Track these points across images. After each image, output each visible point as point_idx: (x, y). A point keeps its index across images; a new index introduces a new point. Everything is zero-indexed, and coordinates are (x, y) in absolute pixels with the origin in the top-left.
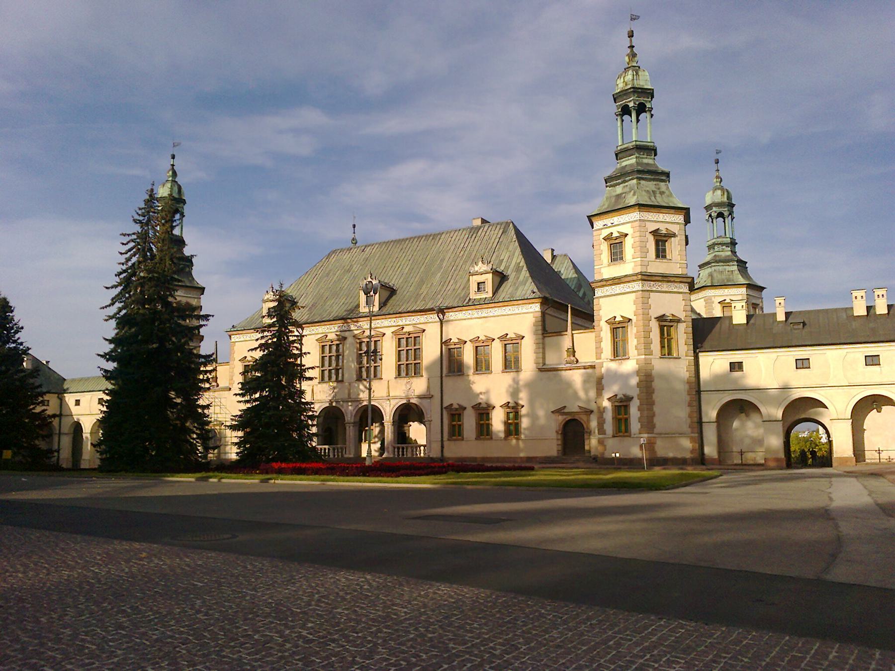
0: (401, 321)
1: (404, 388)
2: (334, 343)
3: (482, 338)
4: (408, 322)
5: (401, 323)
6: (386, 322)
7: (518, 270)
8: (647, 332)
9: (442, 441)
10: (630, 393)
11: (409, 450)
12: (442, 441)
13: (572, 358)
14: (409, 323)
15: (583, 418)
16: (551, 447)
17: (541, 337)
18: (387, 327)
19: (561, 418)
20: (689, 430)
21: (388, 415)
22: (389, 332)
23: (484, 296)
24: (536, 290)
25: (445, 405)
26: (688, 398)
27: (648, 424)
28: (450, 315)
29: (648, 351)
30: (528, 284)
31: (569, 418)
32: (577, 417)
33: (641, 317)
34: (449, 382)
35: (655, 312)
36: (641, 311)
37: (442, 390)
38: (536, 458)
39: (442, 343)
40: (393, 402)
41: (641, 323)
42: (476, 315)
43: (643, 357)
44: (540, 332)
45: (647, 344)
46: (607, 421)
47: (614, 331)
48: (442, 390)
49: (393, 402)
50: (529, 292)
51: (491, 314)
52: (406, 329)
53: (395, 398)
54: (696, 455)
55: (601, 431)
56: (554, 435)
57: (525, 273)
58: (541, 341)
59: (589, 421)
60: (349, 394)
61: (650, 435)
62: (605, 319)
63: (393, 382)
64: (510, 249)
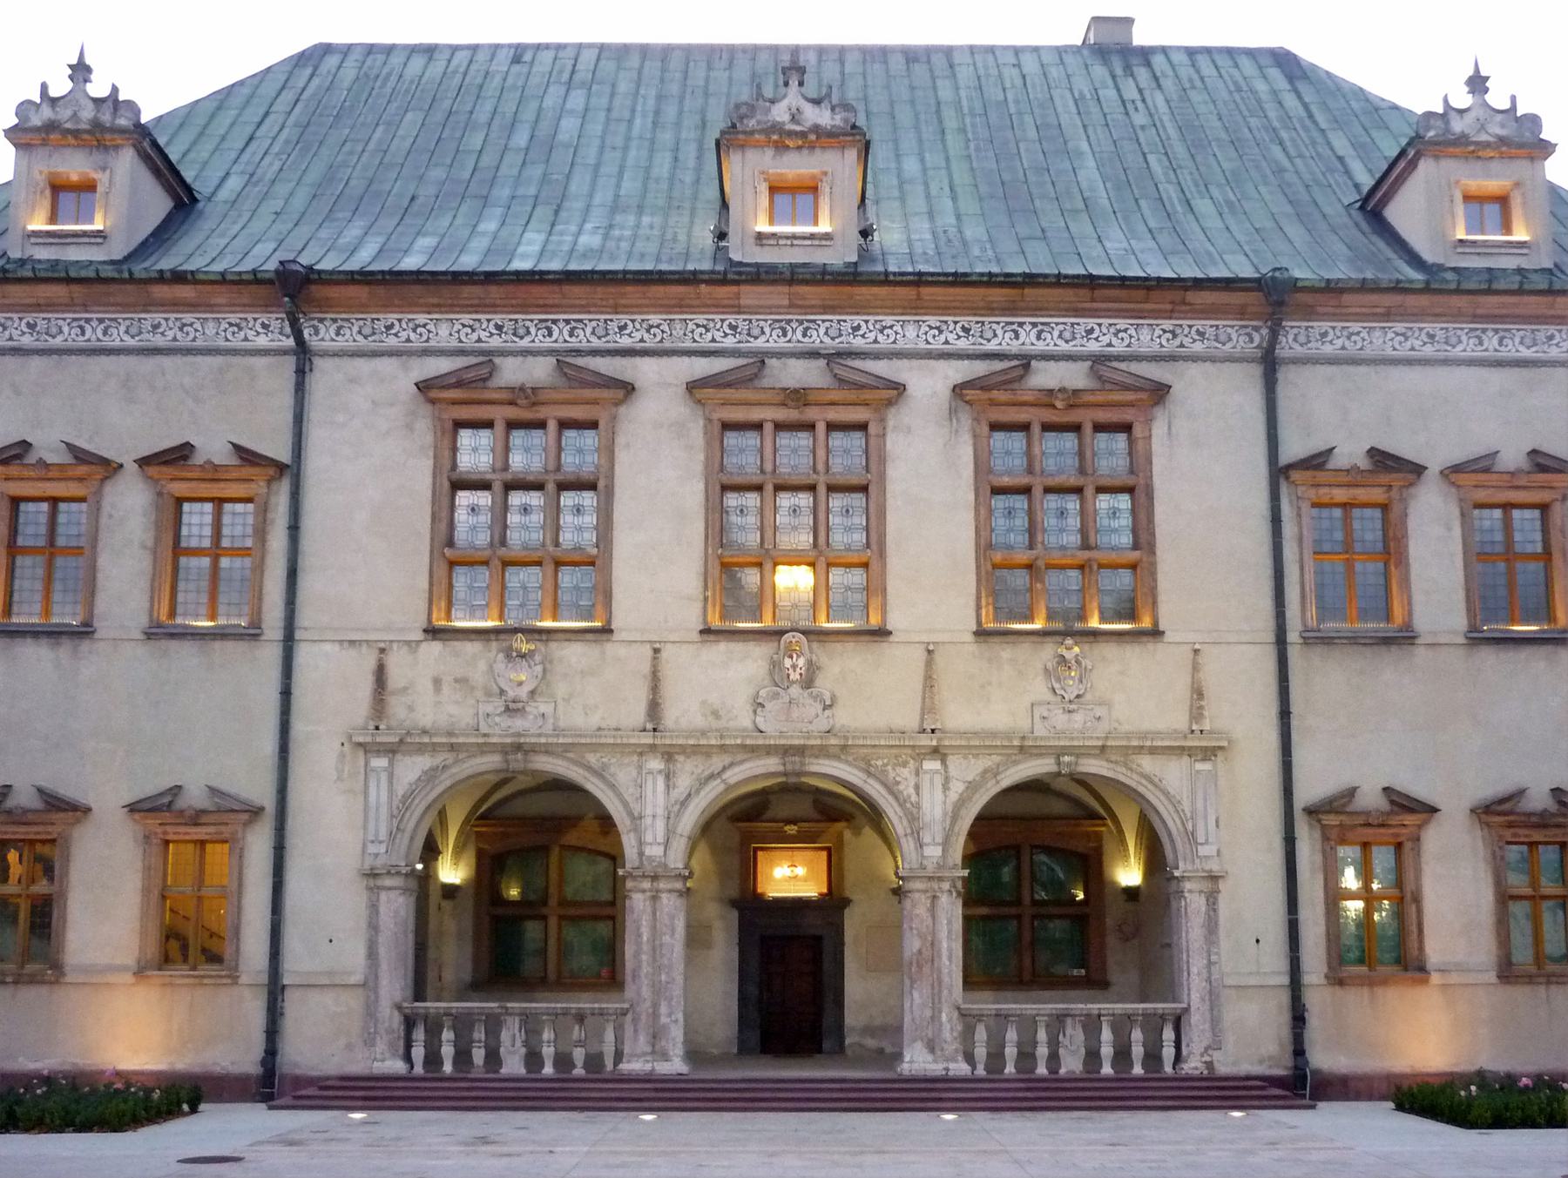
0: (1006, 336)
1: (1039, 689)
4: (1052, 342)
5: (1002, 341)
6: (911, 333)
11: (1074, 1037)
22: (929, 385)
25: (1308, 791)
28: (1296, 338)
37: (1285, 714)
39: (1279, 473)
40: (964, 770)
42: (1467, 347)
48: (1285, 714)
52: (1046, 376)
53: (979, 743)
60: (654, 708)
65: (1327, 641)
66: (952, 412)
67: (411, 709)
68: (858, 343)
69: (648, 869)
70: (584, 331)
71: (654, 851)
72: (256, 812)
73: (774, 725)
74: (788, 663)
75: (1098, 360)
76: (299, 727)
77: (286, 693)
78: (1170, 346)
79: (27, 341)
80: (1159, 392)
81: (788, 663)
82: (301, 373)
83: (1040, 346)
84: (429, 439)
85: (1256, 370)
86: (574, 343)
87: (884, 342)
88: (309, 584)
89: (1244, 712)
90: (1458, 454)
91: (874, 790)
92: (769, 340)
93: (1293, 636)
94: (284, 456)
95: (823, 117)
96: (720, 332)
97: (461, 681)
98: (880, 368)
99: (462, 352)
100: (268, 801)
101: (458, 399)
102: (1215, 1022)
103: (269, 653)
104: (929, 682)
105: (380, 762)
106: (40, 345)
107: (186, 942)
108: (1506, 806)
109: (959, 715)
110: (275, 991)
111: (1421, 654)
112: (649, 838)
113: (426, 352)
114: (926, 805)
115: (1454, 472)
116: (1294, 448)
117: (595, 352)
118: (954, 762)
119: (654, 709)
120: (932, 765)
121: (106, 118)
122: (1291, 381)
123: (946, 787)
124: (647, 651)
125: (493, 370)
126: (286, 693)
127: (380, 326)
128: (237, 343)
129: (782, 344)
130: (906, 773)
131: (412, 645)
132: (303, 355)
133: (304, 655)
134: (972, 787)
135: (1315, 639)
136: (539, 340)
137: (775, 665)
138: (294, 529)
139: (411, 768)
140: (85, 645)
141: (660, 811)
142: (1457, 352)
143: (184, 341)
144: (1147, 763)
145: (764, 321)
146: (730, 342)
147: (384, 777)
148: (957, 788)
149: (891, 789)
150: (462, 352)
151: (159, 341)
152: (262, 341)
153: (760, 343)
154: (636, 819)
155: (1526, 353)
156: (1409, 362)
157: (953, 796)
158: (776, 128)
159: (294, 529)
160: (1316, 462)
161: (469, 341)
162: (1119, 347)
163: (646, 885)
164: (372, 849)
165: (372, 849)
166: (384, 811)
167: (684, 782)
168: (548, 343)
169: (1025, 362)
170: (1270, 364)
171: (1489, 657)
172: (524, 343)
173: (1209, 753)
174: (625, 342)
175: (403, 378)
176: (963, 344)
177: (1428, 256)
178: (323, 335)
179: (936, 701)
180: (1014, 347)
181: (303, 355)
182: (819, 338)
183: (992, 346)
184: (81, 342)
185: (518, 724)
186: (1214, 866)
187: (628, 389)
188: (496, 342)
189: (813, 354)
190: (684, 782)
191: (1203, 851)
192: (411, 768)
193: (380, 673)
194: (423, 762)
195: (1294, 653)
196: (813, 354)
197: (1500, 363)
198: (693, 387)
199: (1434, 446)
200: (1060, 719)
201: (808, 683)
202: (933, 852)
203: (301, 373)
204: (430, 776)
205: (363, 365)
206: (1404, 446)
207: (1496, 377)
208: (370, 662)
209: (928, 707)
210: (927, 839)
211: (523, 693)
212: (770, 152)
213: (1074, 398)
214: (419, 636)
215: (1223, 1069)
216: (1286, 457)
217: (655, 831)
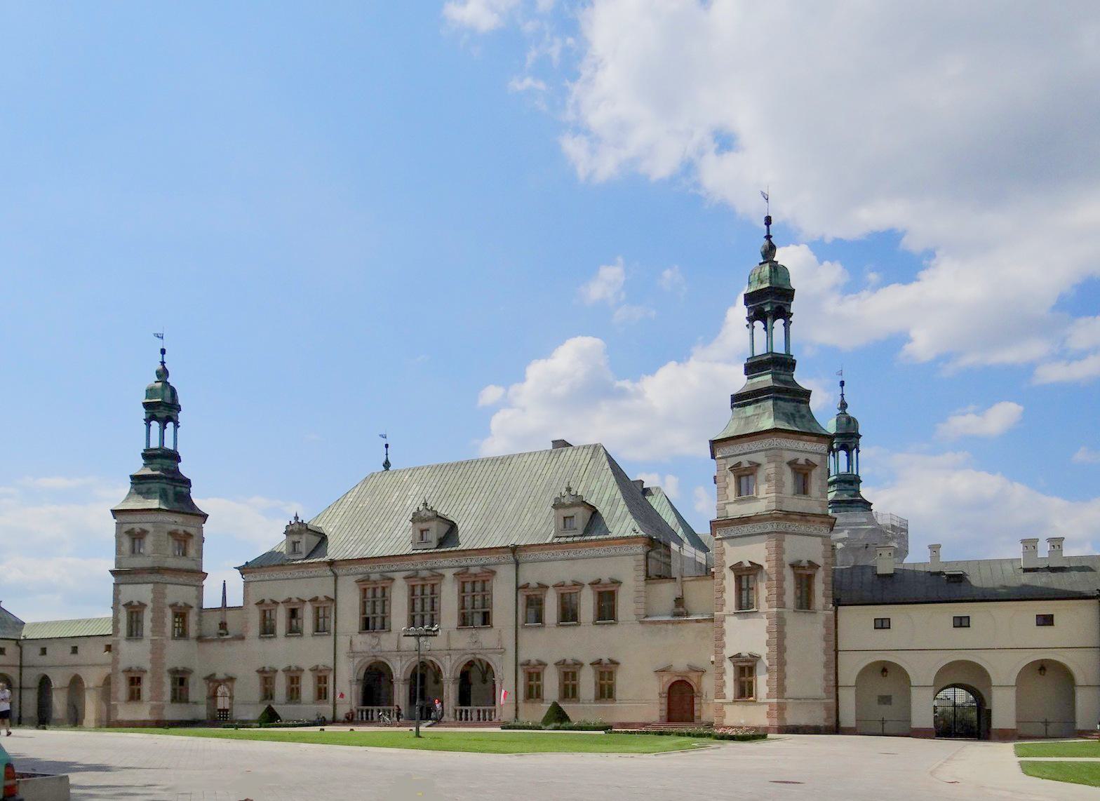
1: (468, 640)
2: (380, 585)
3: (568, 582)
4: (474, 562)
6: (446, 563)
7: (613, 502)
8: (781, 580)
10: (756, 652)
13: (681, 609)
17: (643, 583)
19: (668, 679)
20: (824, 695)
21: (448, 672)
22: (449, 574)
24: (638, 529)
26: (822, 658)
27: (781, 689)
29: (781, 604)
30: (627, 521)
31: (676, 679)
33: (773, 563)
34: (525, 636)
35: (788, 558)
36: (773, 557)
39: (517, 588)
41: (773, 570)
43: (775, 610)
44: (643, 578)
45: (781, 595)
46: (727, 684)
47: (738, 579)
50: (629, 529)
52: (473, 570)
54: (832, 722)
55: (720, 693)
57: (622, 507)
58: (641, 589)
61: (780, 700)
62: (729, 564)
63: (455, 634)
64: (601, 478)
65: (527, 627)
66: (454, 580)
68: (436, 565)
70: (385, 567)
72: (332, 670)
75: (483, 566)
76: (337, 653)
80: (493, 573)
88: (339, 623)
90: (555, 582)
92: (419, 567)
95: (430, 514)
96: (408, 565)
97: (365, 643)
98: (440, 571)
100: (333, 668)
101: (364, 583)
103: (332, 637)
109: (453, 647)
111: (546, 629)
113: (357, 574)
115: (555, 586)
116: (522, 583)
118: (453, 657)
120: (448, 657)
121: (301, 527)
122: (523, 568)
125: (369, 576)
130: (443, 659)
132: (336, 576)
133: (338, 638)
134: (456, 661)
135: (523, 626)
136: (377, 570)
138: (335, 613)
139: (357, 660)
144: (489, 655)
148: (453, 662)
149: (441, 662)
154: (395, 669)
158: (421, 517)
159: (335, 613)
160: (526, 586)
167: (404, 662)
169: (467, 568)
170: (517, 564)
173: (502, 653)
174: (393, 569)
175: (352, 579)
178: (339, 571)
179: (450, 646)
181: (336, 576)
182: (428, 565)
187: (392, 580)
192: (357, 660)
196: (428, 569)
198: (406, 578)
200: (472, 647)
203: (336, 581)
204: (360, 662)
205: (347, 577)
206: (546, 582)
207: (568, 563)
212: (420, 523)
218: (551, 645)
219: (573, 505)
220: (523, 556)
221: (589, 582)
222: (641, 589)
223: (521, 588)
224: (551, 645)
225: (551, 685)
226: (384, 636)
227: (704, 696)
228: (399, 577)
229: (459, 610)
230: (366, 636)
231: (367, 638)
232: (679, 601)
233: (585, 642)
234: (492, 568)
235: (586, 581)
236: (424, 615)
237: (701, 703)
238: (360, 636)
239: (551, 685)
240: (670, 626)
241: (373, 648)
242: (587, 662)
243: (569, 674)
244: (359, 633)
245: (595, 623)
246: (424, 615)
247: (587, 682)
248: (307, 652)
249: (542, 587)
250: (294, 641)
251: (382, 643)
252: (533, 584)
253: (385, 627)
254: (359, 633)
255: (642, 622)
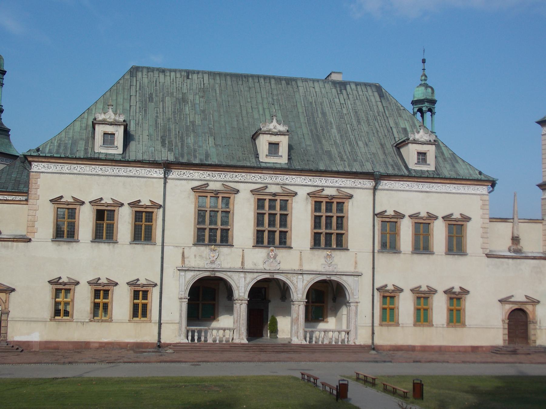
1: (323, 261)
3: (423, 214)
4: (329, 184)
9: (373, 326)
12: (373, 326)
14: (331, 186)
15: (529, 308)
16: (497, 336)
18: (302, 187)
19: (508, 307)
21: (300, 292)
22: (303, 192)
23: (424, 168)
31: (516, 307)
32: (523, 307)
34: (383, 260)
37: (373, 268)
38: (482, 347)
39: (375, 215)
48: (373, 268)
49: (307, 278)
51: (433, 190)
52: (328, 192)
56: (500, 324)
59: (534, 311)
60: (243, 263)
63: (308, 253)
66: (307, 199)
67: (189, 262)
68: (287, 182)
69: (241, 298)
71: (242, 294)
73: (268, 268)
74: (271, 254)
75: (338, 189)
77: (162, 258)
78: (354, 185)
79: (100, 173)
80: (351, 197)
81: (271, 254)
82: (165, 183)
83: (326, 184)
84: (194, 200)
85: (372, 191)
86: (225, 179)
87: (293, 182)
89: (365, 268)
91: (288, 282)
92: (268, 180)
93: (376, 251)
94: (161, 203)
96: (258, 179)
99: (201, 180)
101: (200, 191)
102: (356, 334)
104: (301, 259)
105: (183, 273)
106: (103, 174)
107: (140, 311)
108: (417, 289)
109: (306, 267)
110: (160, 324)
111: (401, 255)
112: (241, 292)
114: (299, 286)
117: (230, 182)
119: (243, 263)
120: (300, 277)
123: (303, 282)
124: (241, 250)
126: (162, 258)
127: (182, 173)
128: (149, 175)
129: (271, 182)
131: (190, 247)
137: (268, 254)
138: (164, 220)
140: (116, 245)
141: (243, 286)
142: (413, 189)
143: (137, 175)
144: (344, 278)
145: (267, 176)
146: (259, 181)
147: (183, 277)
148: (305, 282)
150: (201, 180)
151: (131, 174)
152: (155, 175)
153: (266, 181)
155: (428, 190)
156: (403, 191)
157: (304, 284)
159: (164, 220)
161: (202, 178)
162: (343, 185)
163: (240, 302)
164: (181, 293)
165: (181, 293)
166: (183, 284)
168: (220, 179)
171: (416, 257)
172: (214, 179)
174: (237, 179)
176: (310, 183)
177: (410, 167)
179: (300, 263)
180: (320, 184)
183: (316, 184)
184: (113, 174)
185: (213, 266)
186: (357, 300)
188: (208, 178)
189: (278, 184)
190: (248, 280)
191: (355, 297)
192: (190, 275)
193: (183, 253)
194: (192, 273)
195: (376, 254)
196: (278, 184)
197: (422, 192)
199: (407, 211)
201: (275, 258)
202: (300, 296)
203: (165, 183)
204: (194, 277)
208: (181, 251)
209: (301, 265)
210: (299, 293)
211: (214, 259)
213: (333, 197)
214: (192, 245)
215: (357, 343)
216: (376, 212)
217: (242, 290)
218: (405, 271)
219: (429, 143)
220: (385, 184)
221: (443, 215)
222: (486, 226)
223: (376, 215)
224: (405, 271)
225: (406, 306)
226: (224, 250)
227: (538, 323)
228: (245, 190)
229: (312, 230)
230: (203, 248)
231: (204, 250)
232: (515, 240)
233: (438, 271)
234: (350, 191)
235: (440, 215)
236: (272, 231)
237: (535, 329)
238: (195, 248)
239: (406, 306)
240: (510, 261)
241: (213, 262)
242: (441, 287)
243: (423, 297)
244: (194, 245)
245: (446, 254)
246: (272, 231)
247: (439, 306)
248: (123, 262)
249: (399, 216)
250: (104, 248)
251: (222, 258)
252: (390, 212)
253: (225, 239)
254: (194, 245)
255: (488, 256)
